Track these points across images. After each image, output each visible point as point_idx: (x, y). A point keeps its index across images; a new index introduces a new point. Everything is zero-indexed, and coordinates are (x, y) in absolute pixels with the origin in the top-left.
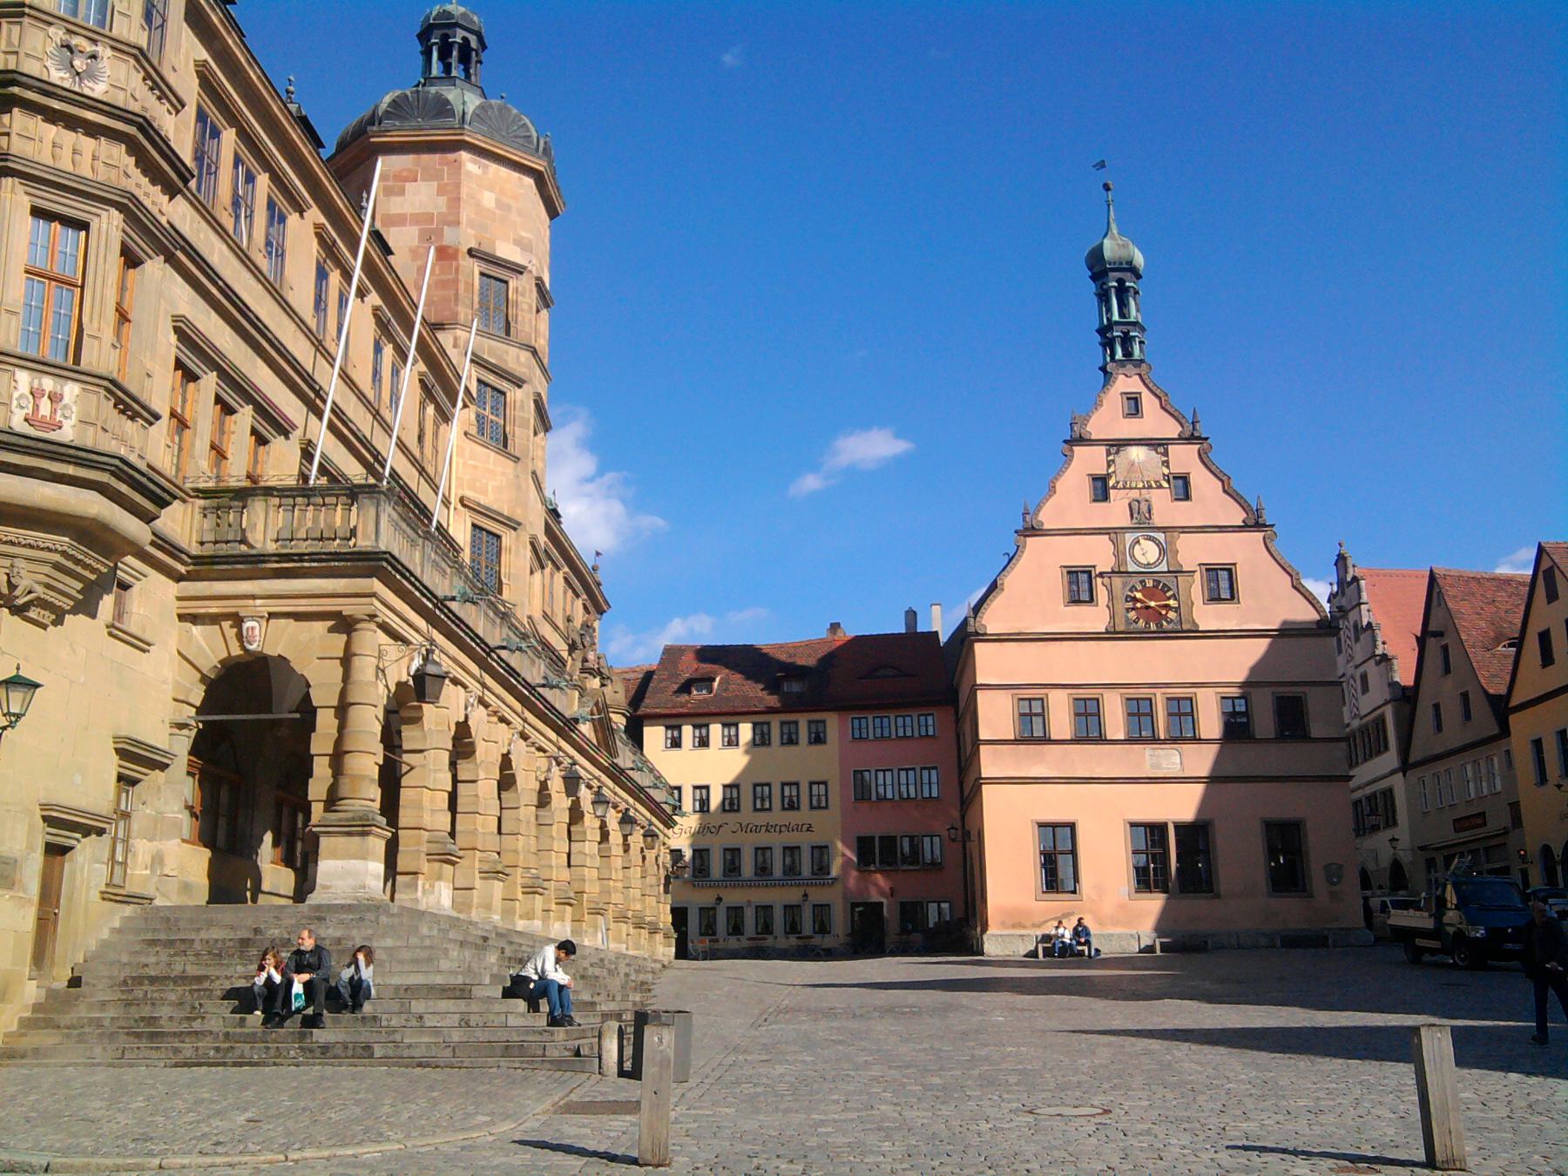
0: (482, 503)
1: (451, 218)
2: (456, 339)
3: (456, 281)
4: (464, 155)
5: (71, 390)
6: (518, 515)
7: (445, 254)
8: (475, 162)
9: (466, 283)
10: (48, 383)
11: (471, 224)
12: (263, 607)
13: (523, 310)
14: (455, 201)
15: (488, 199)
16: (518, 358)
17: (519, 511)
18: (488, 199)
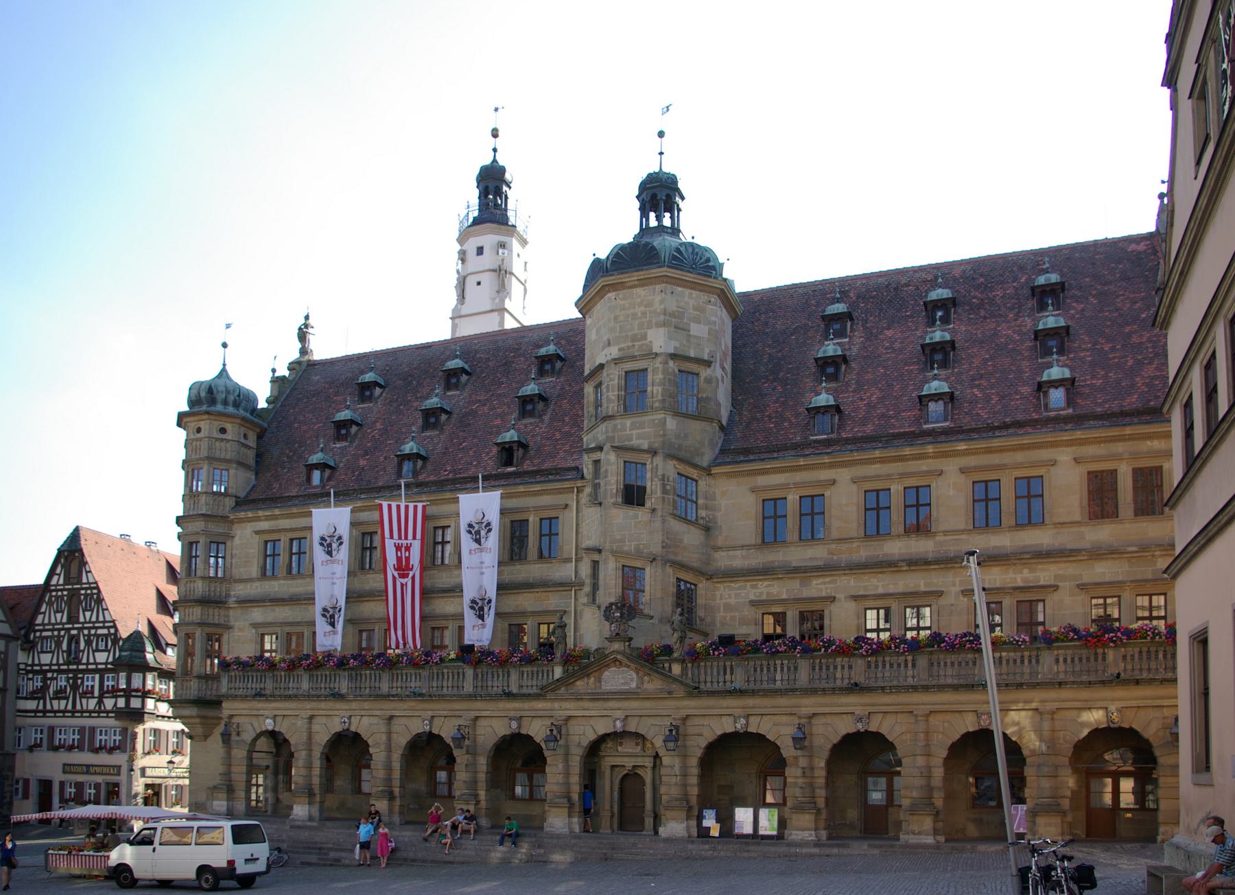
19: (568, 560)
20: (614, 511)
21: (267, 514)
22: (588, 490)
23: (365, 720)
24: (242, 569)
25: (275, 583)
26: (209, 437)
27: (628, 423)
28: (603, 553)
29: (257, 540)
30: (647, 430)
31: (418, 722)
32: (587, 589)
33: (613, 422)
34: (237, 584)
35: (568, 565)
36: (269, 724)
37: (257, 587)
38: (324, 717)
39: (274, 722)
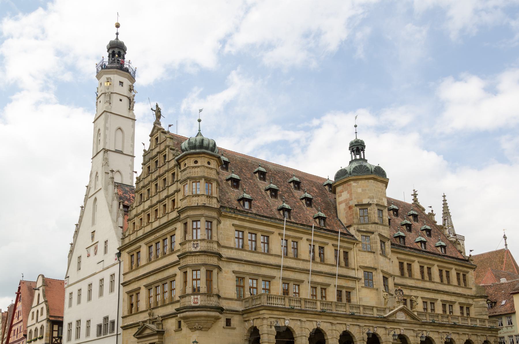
0: (366, 266)
1: (351, 199)
2: (354, 228)
3: (353, 214)
4: (352, 182)
5: (199, 297)
6: (376, 266)
7: (350, 208)
8: (354, 183)
9: (355, 213)
10: (196, 297)
11: (355, 198)
12: (252, 318)
13: (372, 214)
14: (351, 195)
15: (360, 190)
16: (372, 226)
17: (376, 265)
18: (360, 190)
19: (354, 269)
20: (380, 256)
21: (242, 218)
22: (360, 245)
23: (325, 324)
24: (225, 241)
25: (244, 253)
26: (204, 166)
27: (381, 227)
28: (378, 270)
29: (233, 228)
30: (386, 231)
31: (344, 326)
32: (363, 281)
33: (377, 226)
34: (223, 249)
35: (354, 271)
36: (287, 323)
37: (234, 252)
38: (309, 322)
39: (289, 322)
